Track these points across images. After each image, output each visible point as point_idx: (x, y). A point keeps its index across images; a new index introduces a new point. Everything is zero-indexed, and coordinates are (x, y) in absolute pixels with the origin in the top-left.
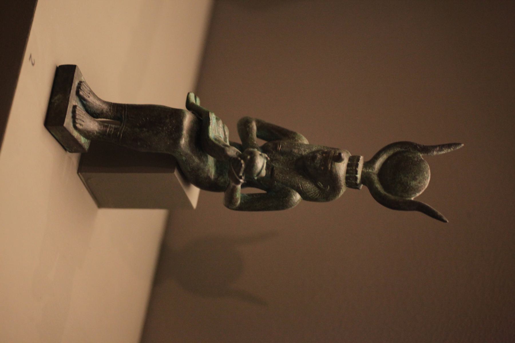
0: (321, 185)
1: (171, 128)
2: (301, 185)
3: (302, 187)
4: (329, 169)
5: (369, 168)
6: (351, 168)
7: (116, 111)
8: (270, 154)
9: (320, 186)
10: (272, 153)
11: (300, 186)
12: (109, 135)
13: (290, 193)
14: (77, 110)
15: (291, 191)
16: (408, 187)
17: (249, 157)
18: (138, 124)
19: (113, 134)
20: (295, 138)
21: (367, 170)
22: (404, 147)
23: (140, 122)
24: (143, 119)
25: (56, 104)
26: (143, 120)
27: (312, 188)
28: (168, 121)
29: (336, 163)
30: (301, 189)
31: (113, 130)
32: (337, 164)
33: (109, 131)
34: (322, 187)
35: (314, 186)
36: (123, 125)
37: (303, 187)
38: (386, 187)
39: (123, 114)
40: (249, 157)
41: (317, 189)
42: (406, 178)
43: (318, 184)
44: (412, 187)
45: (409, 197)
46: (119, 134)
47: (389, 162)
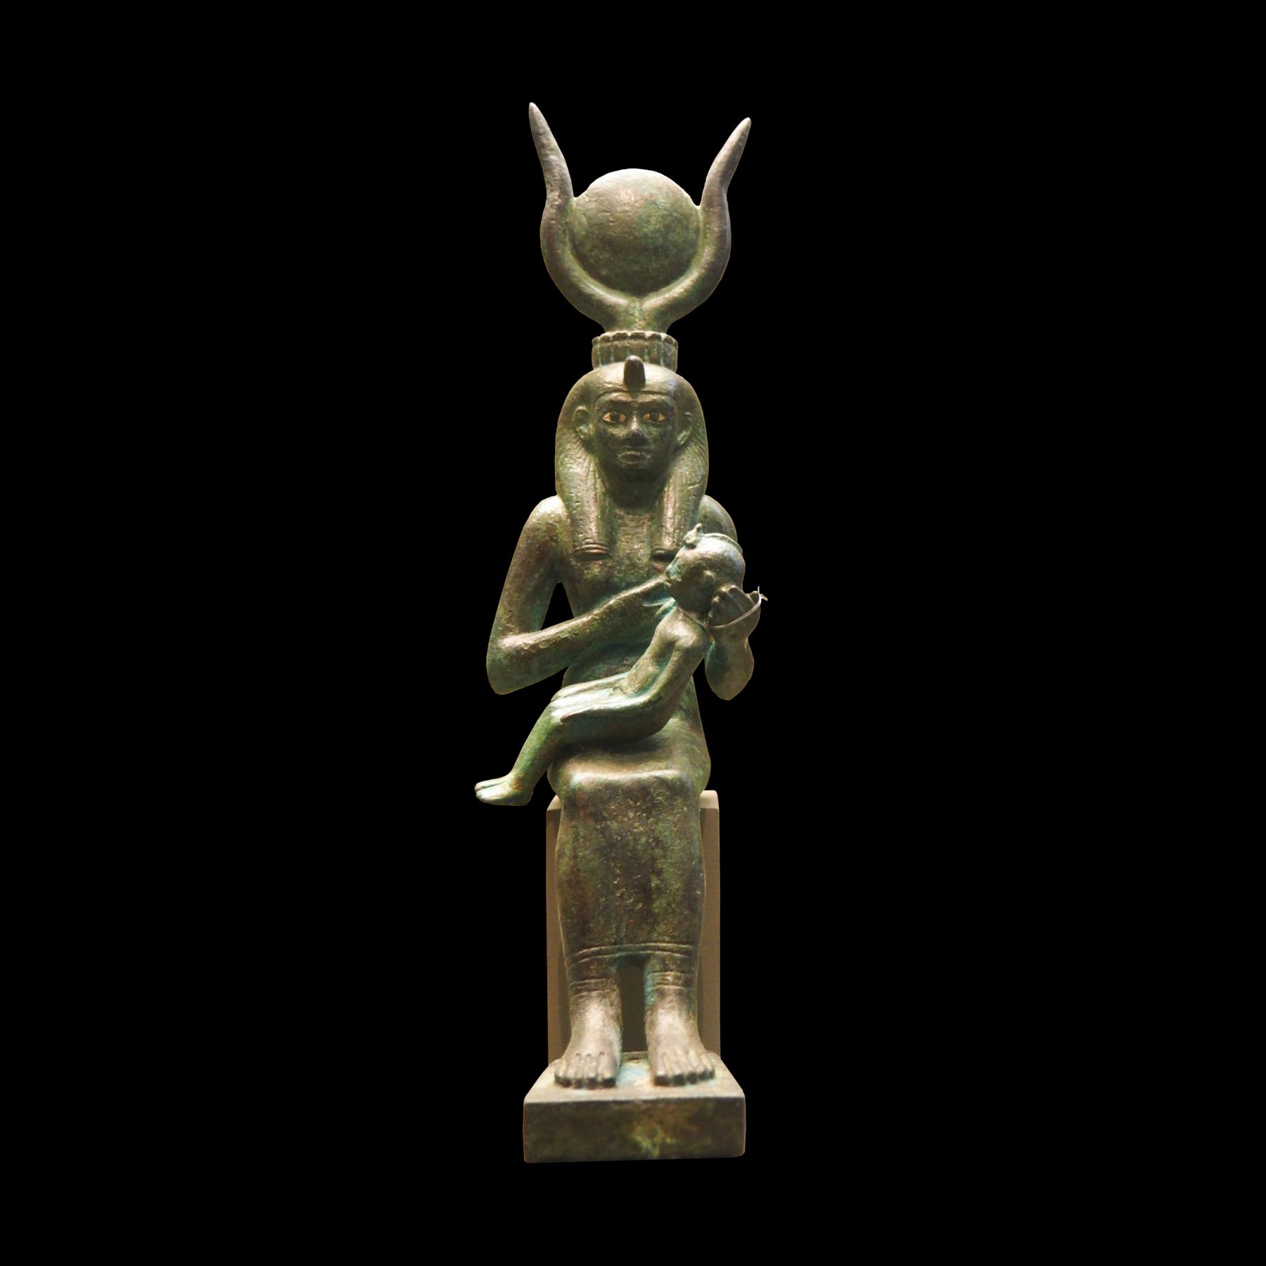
0: (685, 436)
1: (637, 811)
2: (690, 485)
3: (693, 484)
4: (663, 397)
5: (632, 315)
6: (646, 351)
7: (604, 979)
8: (616, 572)
9: (685, 439)
10: (611, 567)
11: (691, 487)
12: (687, 983)
13: (708, 514)
14: (670, 1074)
15: (703, 512)
16: (675, 214)
17: (708, 573)
18: (638, 907)
19: (682, 972)
20: (552, 525)
21: (637, 320)
22: (563, 236)
23: (631, 900)
24: (618, 895)
25: (669, 1140)
26: (622, 894)
27: (690, 459)
28: (614, 825)
29: (647, 382)
30: (697, 485)
31: (672, 973)
32: (649, 380)
33: (677, 985)
34: (689, 433)
35: (683, 457)
36: (646, 948)
37: (693, 482)
38: (678, 270)
39: (611, 956)
40: (708, 573)
41: (688, 448)
42: (653, 221)
43: (682, 442)
44: (672, 205)
45: (697, 214)
46: (682, 953)
47: (604, 273)
